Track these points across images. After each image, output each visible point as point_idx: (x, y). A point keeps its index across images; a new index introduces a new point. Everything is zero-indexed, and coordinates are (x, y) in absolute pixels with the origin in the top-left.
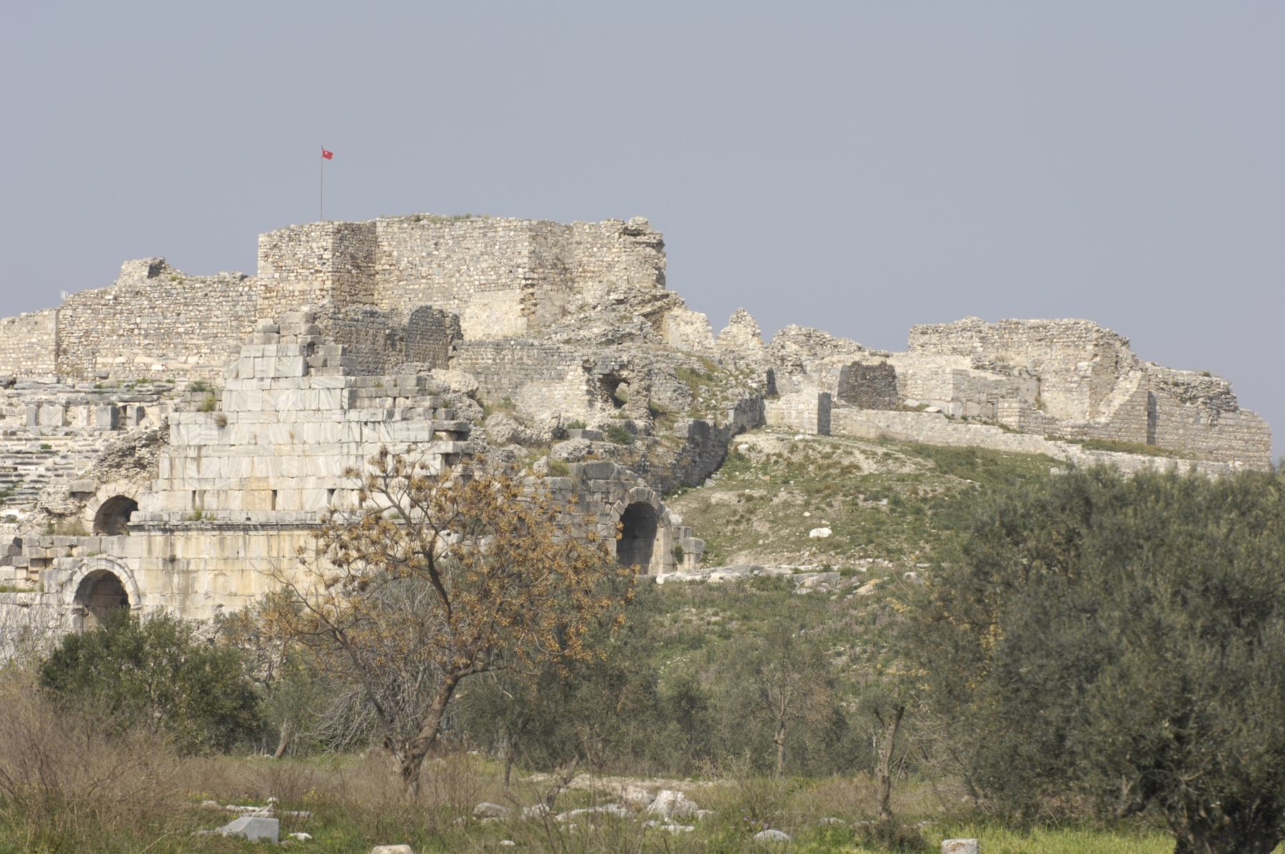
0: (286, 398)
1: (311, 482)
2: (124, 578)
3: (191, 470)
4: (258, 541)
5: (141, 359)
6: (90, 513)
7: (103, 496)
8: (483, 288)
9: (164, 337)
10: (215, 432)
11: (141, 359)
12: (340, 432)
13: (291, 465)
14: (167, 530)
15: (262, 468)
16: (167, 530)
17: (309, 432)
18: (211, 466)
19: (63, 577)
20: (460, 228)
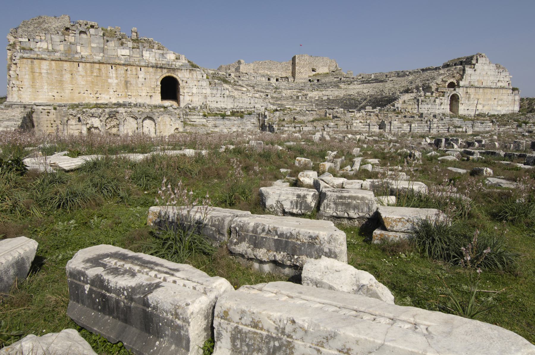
0: (486, 67)
1: (489, 81)
2: (459, 95)
3: (469, 78)
4: (481, 90)
5: (266, 72)
6: (447, 84)
7: (449, 82)
8: (322, 66)
9: (270, 69)
10: (474, 72)
11: (266, 72)
12: (494, 73)
13: (486, 78)
14: (467, 87)
15: (481, 78)
16: (467, 87)
17: (489, 73)
18: (472, 78)
19: (448, 94)
20: (318, 58)
